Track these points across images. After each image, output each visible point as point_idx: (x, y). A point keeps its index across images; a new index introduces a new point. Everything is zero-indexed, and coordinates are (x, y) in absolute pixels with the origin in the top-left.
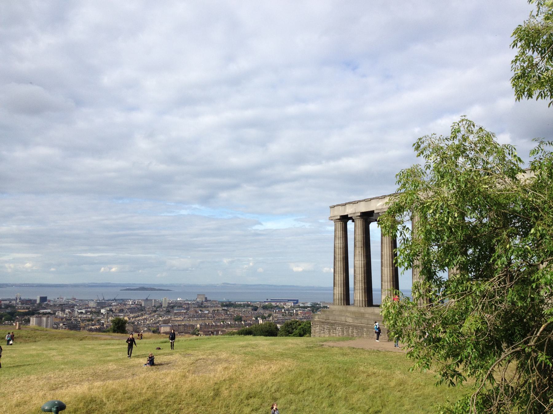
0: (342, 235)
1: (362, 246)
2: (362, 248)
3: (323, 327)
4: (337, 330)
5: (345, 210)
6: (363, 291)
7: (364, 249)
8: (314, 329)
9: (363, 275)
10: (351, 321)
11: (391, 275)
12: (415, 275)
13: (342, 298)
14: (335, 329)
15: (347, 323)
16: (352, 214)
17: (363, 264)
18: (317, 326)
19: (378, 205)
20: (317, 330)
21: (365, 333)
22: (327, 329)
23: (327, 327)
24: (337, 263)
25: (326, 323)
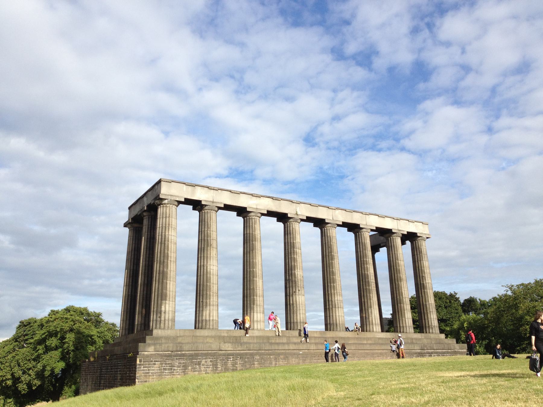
3: (169, 364)
4: (203, 365)
5: (193, 193)
8: (143, 370)
10: (229, 349)
12: (299, 290)
14: (199, 364)
15: (221, 352)
16: (207, 201)
18: (155, 364)
20: (154, 370)
21: (256, 363)
22: (179, 367)
23: (180, 363)
24: (172, 264)
25: (175, 356)
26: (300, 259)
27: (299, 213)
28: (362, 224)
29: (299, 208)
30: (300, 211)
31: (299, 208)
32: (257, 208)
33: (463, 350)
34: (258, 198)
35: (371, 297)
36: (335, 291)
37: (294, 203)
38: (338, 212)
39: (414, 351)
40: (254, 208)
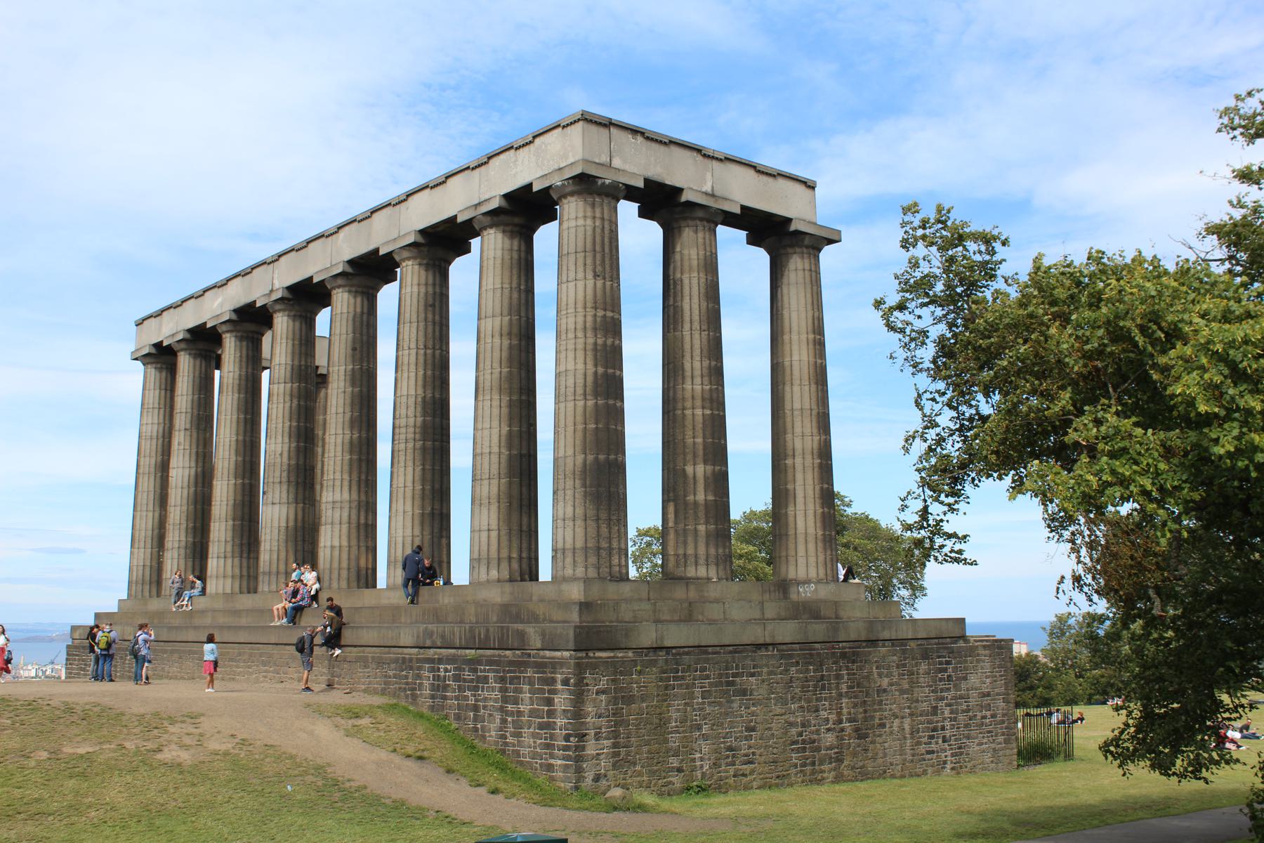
0: (157, 401)
1: (188, 426)
2: (188, 433)
6: (183, 552)
7: (191, 436)
9: (185, 508)
11: (231, 502)
13: (147, 578)
17: (186, 479)
26: (274, 411)
33: (558, 654)
39: (400, 650)
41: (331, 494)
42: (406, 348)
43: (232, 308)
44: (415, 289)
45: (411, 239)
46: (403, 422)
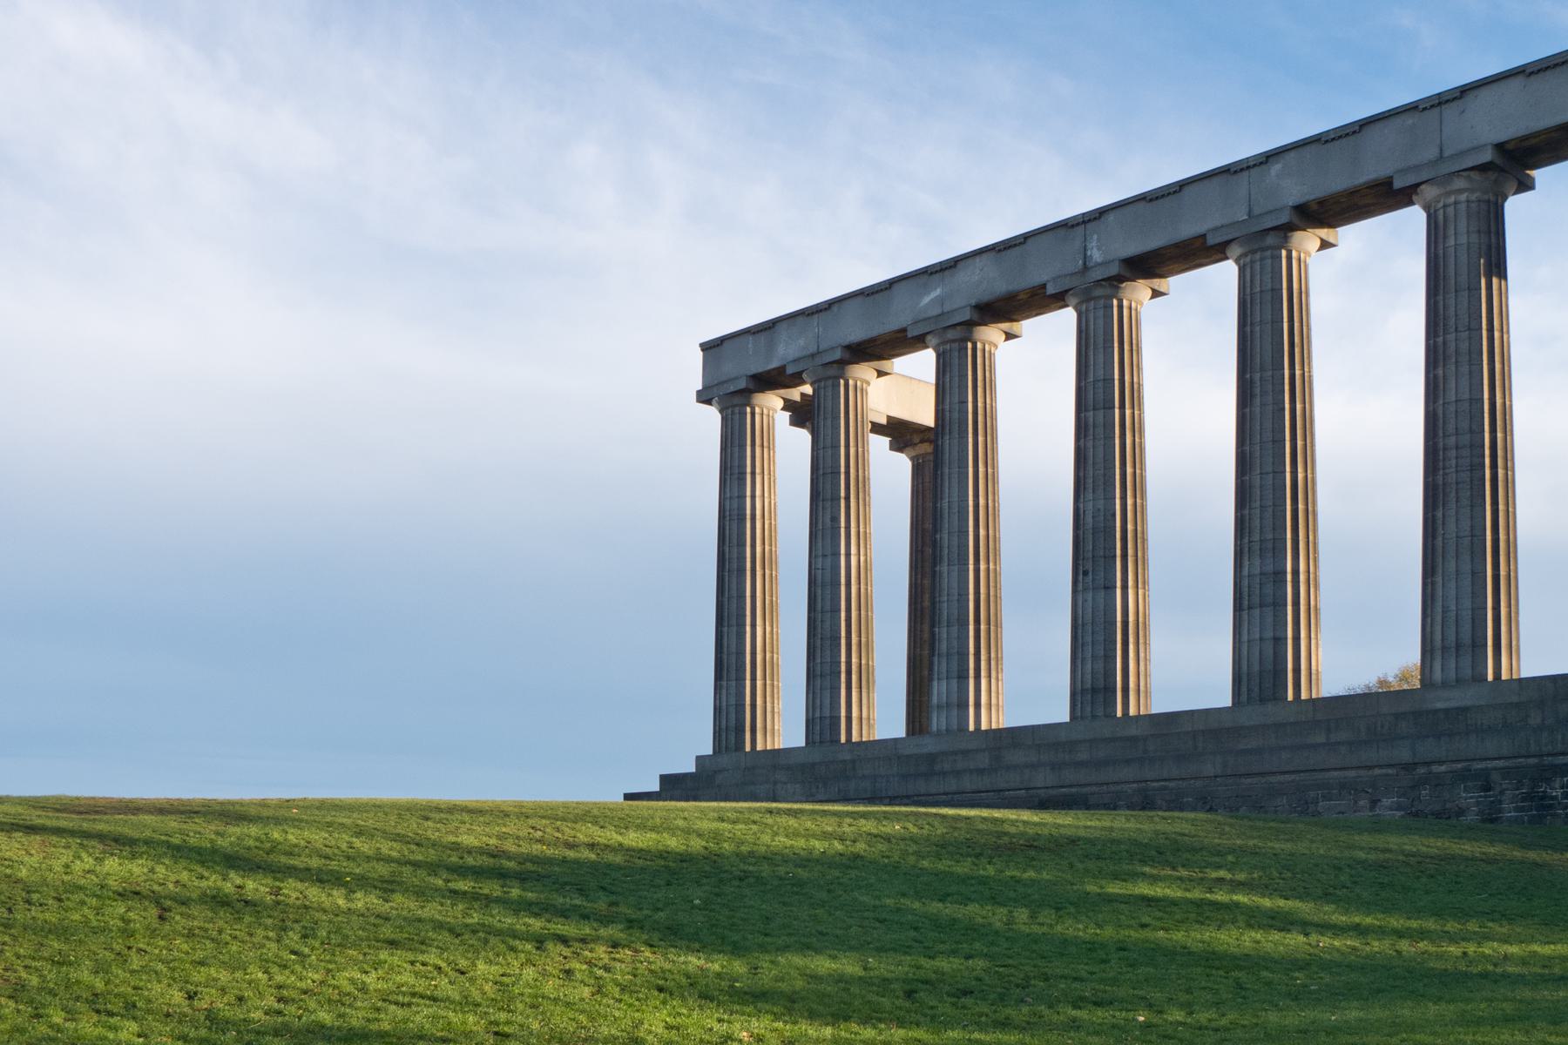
19: (926, 300)
27: (1096, 255)
28: (1403, 171)
29: (1095, 237)
30: (1099, 249)
31: (1095, 237)
32: (943, 314)
34: (947, 273)
35: (1440, 522)
36: (1246, 540)
37: (1073, 226)
38: (1276, 168)
40: (929, 318)
41: (1257, 562)
42: (1453, 330)
43: (973, 302)
44: (1474, 238)
45: (1487, 156)
46: (1452, 441)
